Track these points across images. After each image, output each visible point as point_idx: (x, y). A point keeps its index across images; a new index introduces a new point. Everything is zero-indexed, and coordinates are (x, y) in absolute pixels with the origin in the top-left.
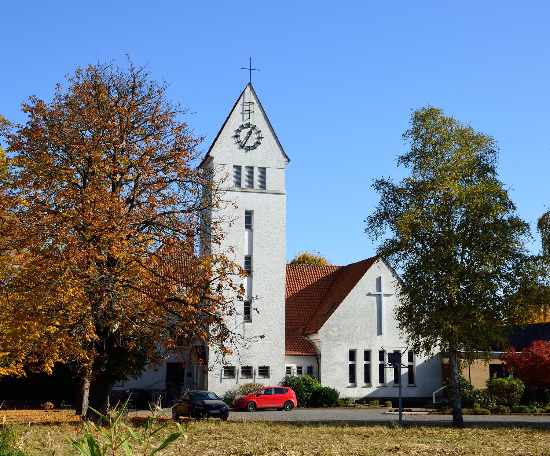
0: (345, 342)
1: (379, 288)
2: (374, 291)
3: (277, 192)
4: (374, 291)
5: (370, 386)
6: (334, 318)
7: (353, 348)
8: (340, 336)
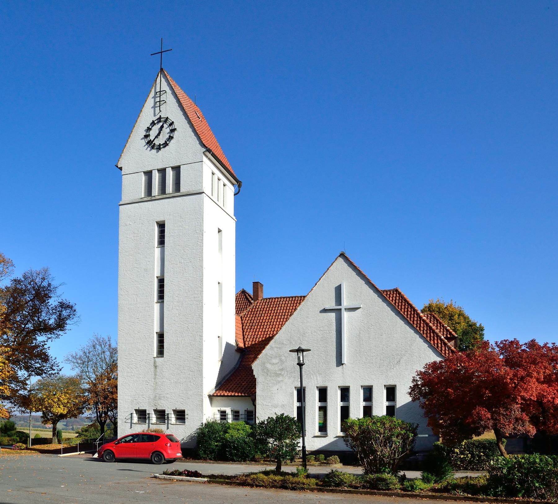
0: (289, 378)
1: (339, 300)
2: (332, 305)
3: (195, 192)
4: (332, 305)
5: (326, 436)
6: (273, 346)
7: (391, 383)
8: (282, 370)
